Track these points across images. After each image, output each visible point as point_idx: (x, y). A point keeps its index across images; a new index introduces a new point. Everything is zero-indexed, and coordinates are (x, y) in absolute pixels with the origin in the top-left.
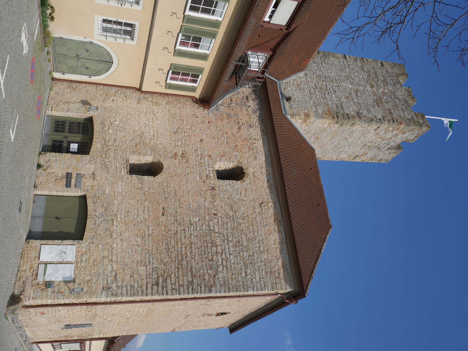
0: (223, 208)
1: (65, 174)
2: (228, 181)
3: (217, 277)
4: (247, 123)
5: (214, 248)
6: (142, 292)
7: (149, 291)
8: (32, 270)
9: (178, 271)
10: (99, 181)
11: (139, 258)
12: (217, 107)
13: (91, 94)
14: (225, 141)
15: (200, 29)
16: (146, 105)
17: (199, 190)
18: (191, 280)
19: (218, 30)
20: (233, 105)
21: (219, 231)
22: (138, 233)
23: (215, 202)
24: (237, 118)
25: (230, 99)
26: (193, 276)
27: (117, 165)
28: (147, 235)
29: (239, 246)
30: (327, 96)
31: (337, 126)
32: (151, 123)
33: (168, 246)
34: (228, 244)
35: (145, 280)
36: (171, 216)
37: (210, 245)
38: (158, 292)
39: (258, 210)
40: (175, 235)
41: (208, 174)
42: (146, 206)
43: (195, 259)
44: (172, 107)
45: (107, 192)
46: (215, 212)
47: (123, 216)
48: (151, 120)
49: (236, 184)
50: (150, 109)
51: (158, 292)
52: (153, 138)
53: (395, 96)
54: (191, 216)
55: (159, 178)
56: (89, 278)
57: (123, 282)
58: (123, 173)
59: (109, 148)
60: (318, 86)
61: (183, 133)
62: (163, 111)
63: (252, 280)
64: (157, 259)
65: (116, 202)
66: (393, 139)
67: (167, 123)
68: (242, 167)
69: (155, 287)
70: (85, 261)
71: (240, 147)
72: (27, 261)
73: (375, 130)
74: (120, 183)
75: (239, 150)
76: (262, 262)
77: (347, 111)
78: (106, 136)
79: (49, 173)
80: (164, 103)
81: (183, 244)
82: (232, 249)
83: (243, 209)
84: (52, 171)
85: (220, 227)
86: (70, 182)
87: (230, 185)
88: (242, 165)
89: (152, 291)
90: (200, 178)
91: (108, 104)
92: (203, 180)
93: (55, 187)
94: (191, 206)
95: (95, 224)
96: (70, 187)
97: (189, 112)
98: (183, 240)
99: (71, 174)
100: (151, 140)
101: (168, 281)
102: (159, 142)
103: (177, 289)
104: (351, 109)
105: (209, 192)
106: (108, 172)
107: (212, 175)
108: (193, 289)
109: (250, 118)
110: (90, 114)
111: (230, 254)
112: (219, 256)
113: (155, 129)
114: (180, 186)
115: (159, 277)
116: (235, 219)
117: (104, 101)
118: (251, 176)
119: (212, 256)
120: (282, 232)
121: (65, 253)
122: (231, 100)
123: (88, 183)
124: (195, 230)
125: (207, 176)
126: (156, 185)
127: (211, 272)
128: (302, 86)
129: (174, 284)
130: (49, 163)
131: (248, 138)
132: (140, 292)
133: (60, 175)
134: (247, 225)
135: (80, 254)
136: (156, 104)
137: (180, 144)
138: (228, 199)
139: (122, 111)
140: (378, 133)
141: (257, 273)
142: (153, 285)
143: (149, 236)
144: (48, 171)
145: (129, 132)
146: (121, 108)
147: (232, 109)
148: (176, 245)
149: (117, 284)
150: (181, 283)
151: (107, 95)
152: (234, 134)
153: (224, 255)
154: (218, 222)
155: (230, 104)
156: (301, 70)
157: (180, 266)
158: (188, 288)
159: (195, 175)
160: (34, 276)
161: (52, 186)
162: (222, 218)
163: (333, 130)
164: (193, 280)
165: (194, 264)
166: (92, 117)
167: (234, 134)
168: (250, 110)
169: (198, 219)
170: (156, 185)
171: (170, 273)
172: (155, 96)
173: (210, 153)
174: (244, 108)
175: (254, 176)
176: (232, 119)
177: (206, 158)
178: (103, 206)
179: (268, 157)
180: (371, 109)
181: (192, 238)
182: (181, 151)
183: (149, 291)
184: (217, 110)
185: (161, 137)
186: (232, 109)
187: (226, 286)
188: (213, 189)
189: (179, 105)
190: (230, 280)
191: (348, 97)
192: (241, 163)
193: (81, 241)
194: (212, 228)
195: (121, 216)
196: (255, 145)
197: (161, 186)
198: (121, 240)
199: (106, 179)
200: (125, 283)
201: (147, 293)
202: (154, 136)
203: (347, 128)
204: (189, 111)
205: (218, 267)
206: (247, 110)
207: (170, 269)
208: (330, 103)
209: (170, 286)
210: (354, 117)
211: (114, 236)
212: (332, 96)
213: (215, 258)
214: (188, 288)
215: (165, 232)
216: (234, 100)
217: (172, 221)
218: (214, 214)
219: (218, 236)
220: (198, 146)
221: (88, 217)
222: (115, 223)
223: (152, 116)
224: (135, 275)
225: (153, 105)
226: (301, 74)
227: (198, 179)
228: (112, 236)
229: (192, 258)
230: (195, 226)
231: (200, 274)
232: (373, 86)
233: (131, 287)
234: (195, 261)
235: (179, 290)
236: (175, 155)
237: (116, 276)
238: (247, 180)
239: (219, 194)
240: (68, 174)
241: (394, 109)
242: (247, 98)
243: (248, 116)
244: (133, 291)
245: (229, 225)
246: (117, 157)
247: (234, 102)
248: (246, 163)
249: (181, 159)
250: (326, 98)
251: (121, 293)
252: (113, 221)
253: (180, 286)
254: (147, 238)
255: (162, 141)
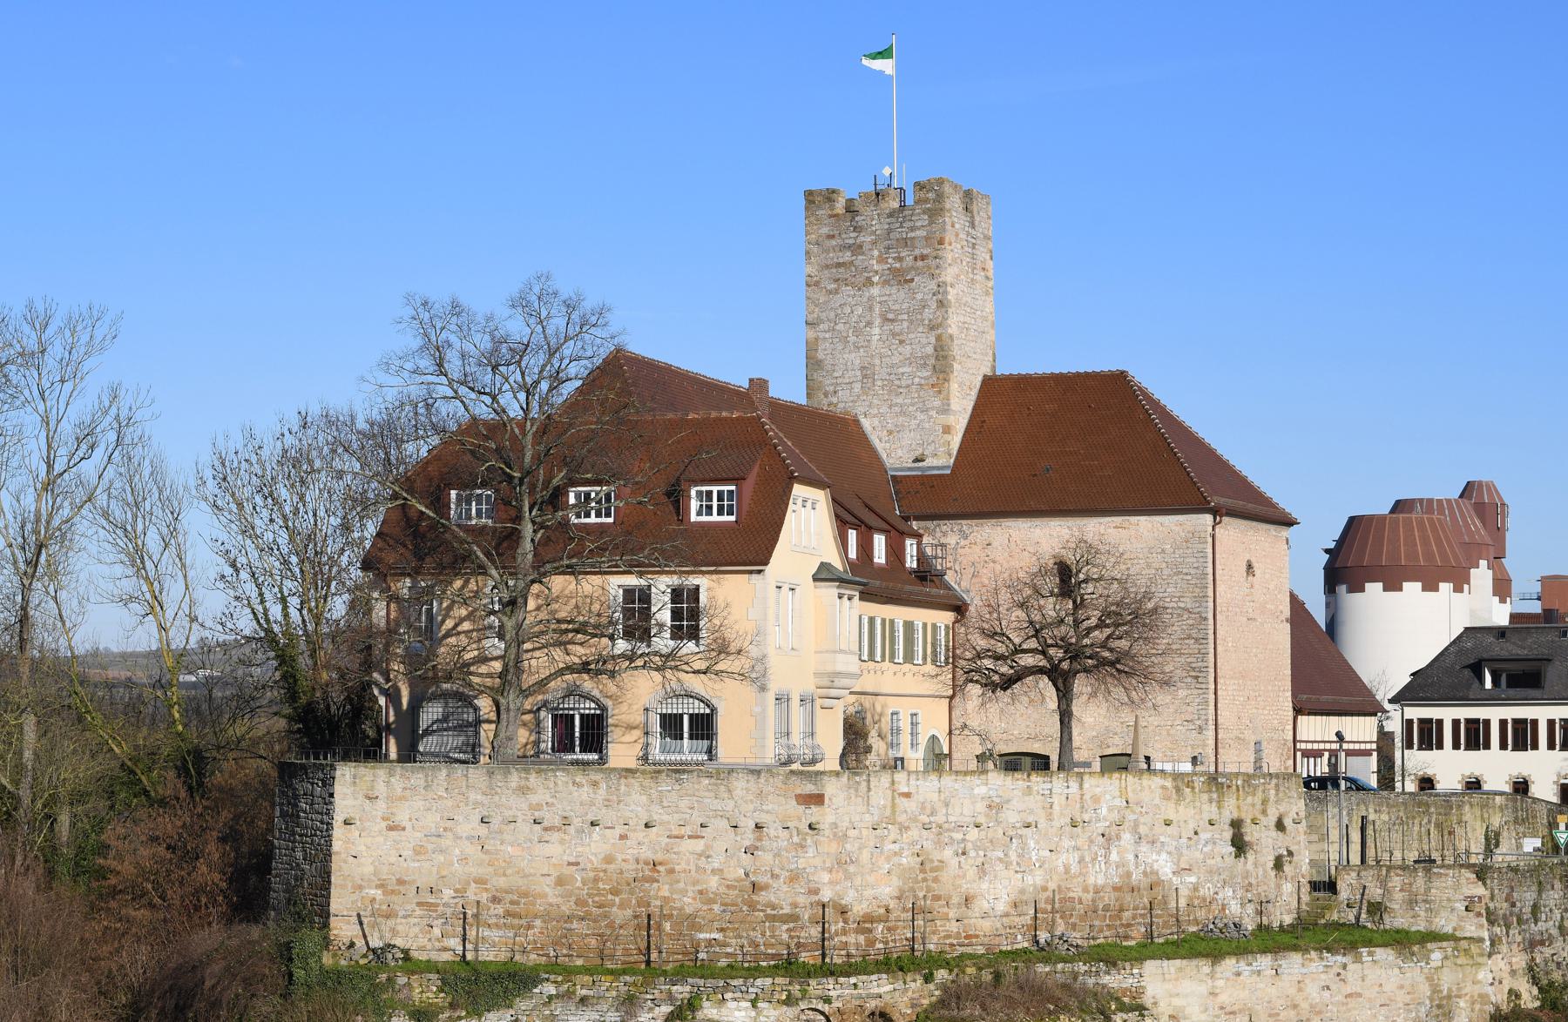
30: (904, 383)
77: (930, 350)
104: (924, 343)
156: (857, 422)
180: (919, 296)
191: (901, 342)
208: (917, 380)
210: (939, 338)
226: (866, 424)
232: (869, 279)
241: (914, 247)
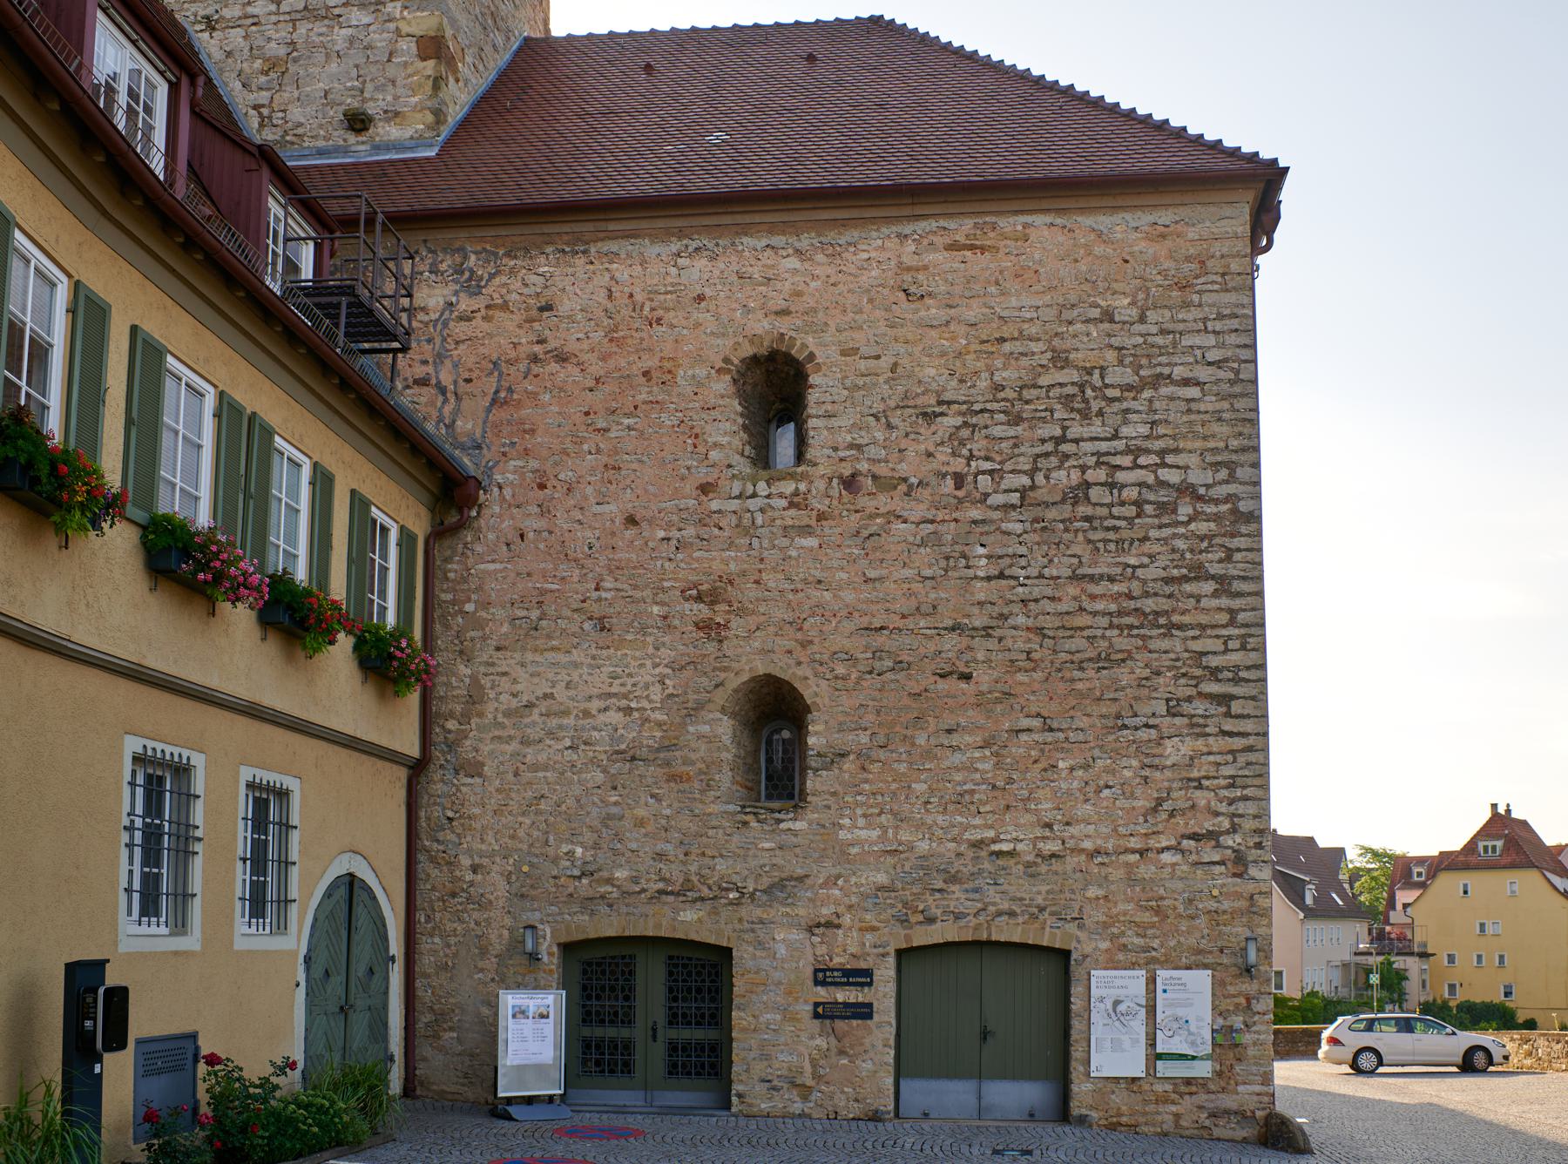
1: (817, 1022)
3: (1202, 491)
4: (530, 321)
5: (1094, 493)
6: (1250, 749)
7: (1248, 726)
8: (1173, 1096)
9: (1180, 627)
10: (841, 910)
11: (1135, 763)
13: (455, 955)
16: (481, 743)
17: (859, 541)
18: (1211, 582)
22: (1040, 766)
23: (905, 480)
26: (1198, 573)
27: (767, 845)
28: (1049, 737)
29: (1086, 401)
32: (569, 721)
33: (1090, 660)
34: (1076, 441)
35: (1211, 740)
36: (970, 648)
37: (1083, 510)
38: (1253, 698)
39: (934, 312)
40: (1044, 636)
41: (784, 503)
42: (933, 741)
43: (1134, 567)
44: (484, 638)
45: (882, 878)
46: (950, 482)
47: (977, 821)
48: (554, 722)
49: (822, 389)
50: (502, 726)
51: (1253, 698)
54: (970, 573)
55: (813, 690)
56: (1202, 922)
57: (1217, 814)
58: (799, 825)
59: (695, 879)
61: (604, 595)
63: (1209, 364)
64: (1136, 699)
65: (923, 846)
67: (562, 658)
68: (743, 361)
69: (1236, 707)
70: (1144, 936)
71: (650, 362)
72: (1145, 1114)
74: (842, 835)
75: (668, 365)
76: (1142, 319)
78: (644, 890)
79: (817, 1077)
80: (464, 670)
81: (1081, 609)
82: (1096, 429)
83: (932, 372)
84: (808, 1068)
85: (1008, 466)
86: (846, 1005)
88: (736, 362)
89: (1249, 716)
90: (806, 530)
91: (496, 886)
92: (813, 522)
93: (871, 1054)
94: (928, 573)
95: (1012, 914)
96: (870, 1005)
97: (498, 566)
98: (1063, 607)
99: (816, 1005)
100: (647, 720)
101: (1214, 661)
102: (658, 687)
103: (1243, 631)
106: (801, 879)
108: (1244, 578)
109: (505, 307)
110: (550, 954)
111: (1115, 437)
112: (1121, 476)
113: (595, 705)
114: (844, 613)
115: (1200, 694)
116: (977, 407)
117: (483, 904)
118: (784, 325)
119: (1122, 504)
121: (1117, 1003)
123: (847, 948)
124: (1023, 562)
125: (792, 505)
126: (847, 702)
127: (1184, 511)
129: (1225, 643)
130: (775, 1083)
131: (606, 322)
132: (1252, 757)
133: (821, 1042)
135: (1121, 957)
136: (475, 698)
137: (656, 609)
139: (521, 833)
141: (1187, 341)
142: (1228, 714)
143: (1051, 730)
144: (809, 1082)
145: (616, 804)
146: (512, 837)
147: (469, 381)
148: (1086, 633)
149: (1227, 832)
150: (1223, 618)
151: (454, 895)
152: (592, 383)
153: (1118, 460)
155: (443, 391)
157: (1162, 621)
158: (1239, 595)
159: (794, 553)
160: (1194, 1089)
161: (868, 1065)
164: (1213, 577)
165: (1153, 572)
166: (559, 945)
167: (592, 383)
170: (847, 702)
171: (1186, 655)
173: (689, 487)
174: (460, 329)
175: (784, 312)
176: (518, 388)
177: (714, 505)
178: (939, 891)
179: (694, 245)
181: (1055, 573)
182: (687, 605)
183: (1248, 726)
184: (479, 447)
186: (469, 381)
187: (1234, 457)
188: (850, 483)
189: (469, 607)
190: (1211, 444)
192: (726, 360)
193: (1074, 956)
194: (1014, 498)
195: (975, 827)
196: (639, 297)
197: (850, 684)
198: (1068, 824)
199: (831, 881)
200: (1223, 808)
201: (1257, 734)
202: (628, 711)
204: (492, 567)
205: (1162, 484)
207: (1172, 656)
209: (1235, 658)
211: (1051, 847)
213: (1131, 493)
214: (1239, 595)
215: (1034, 670)
217: (992, 644)
218: (958, 486)
219: (1047, 477)
220: (661, 534)
221: (984, 937)
222: (1005, 847)
223: (535, 716)
224: (1195, 774)
225: (481, 715)
227: (811, 542)
228: (1053, 855)
229: (1133, 576)
230: (1007, 561)
231: (1192, 551)
233: (1232, 786)
234: (1142, 566)
235: (1247, 626)
237: (1195, 837)
238: (804, 346)
240: (816, 1016)
243: (498, 314)
244: (1249, 781)
246: (732, 847)
247: (430, 369)
248: (729, 343)
251: (1255, 817)
252: (999, 854)
253: (1232, 622)
254: (1061, 735)
255: (648, 678)
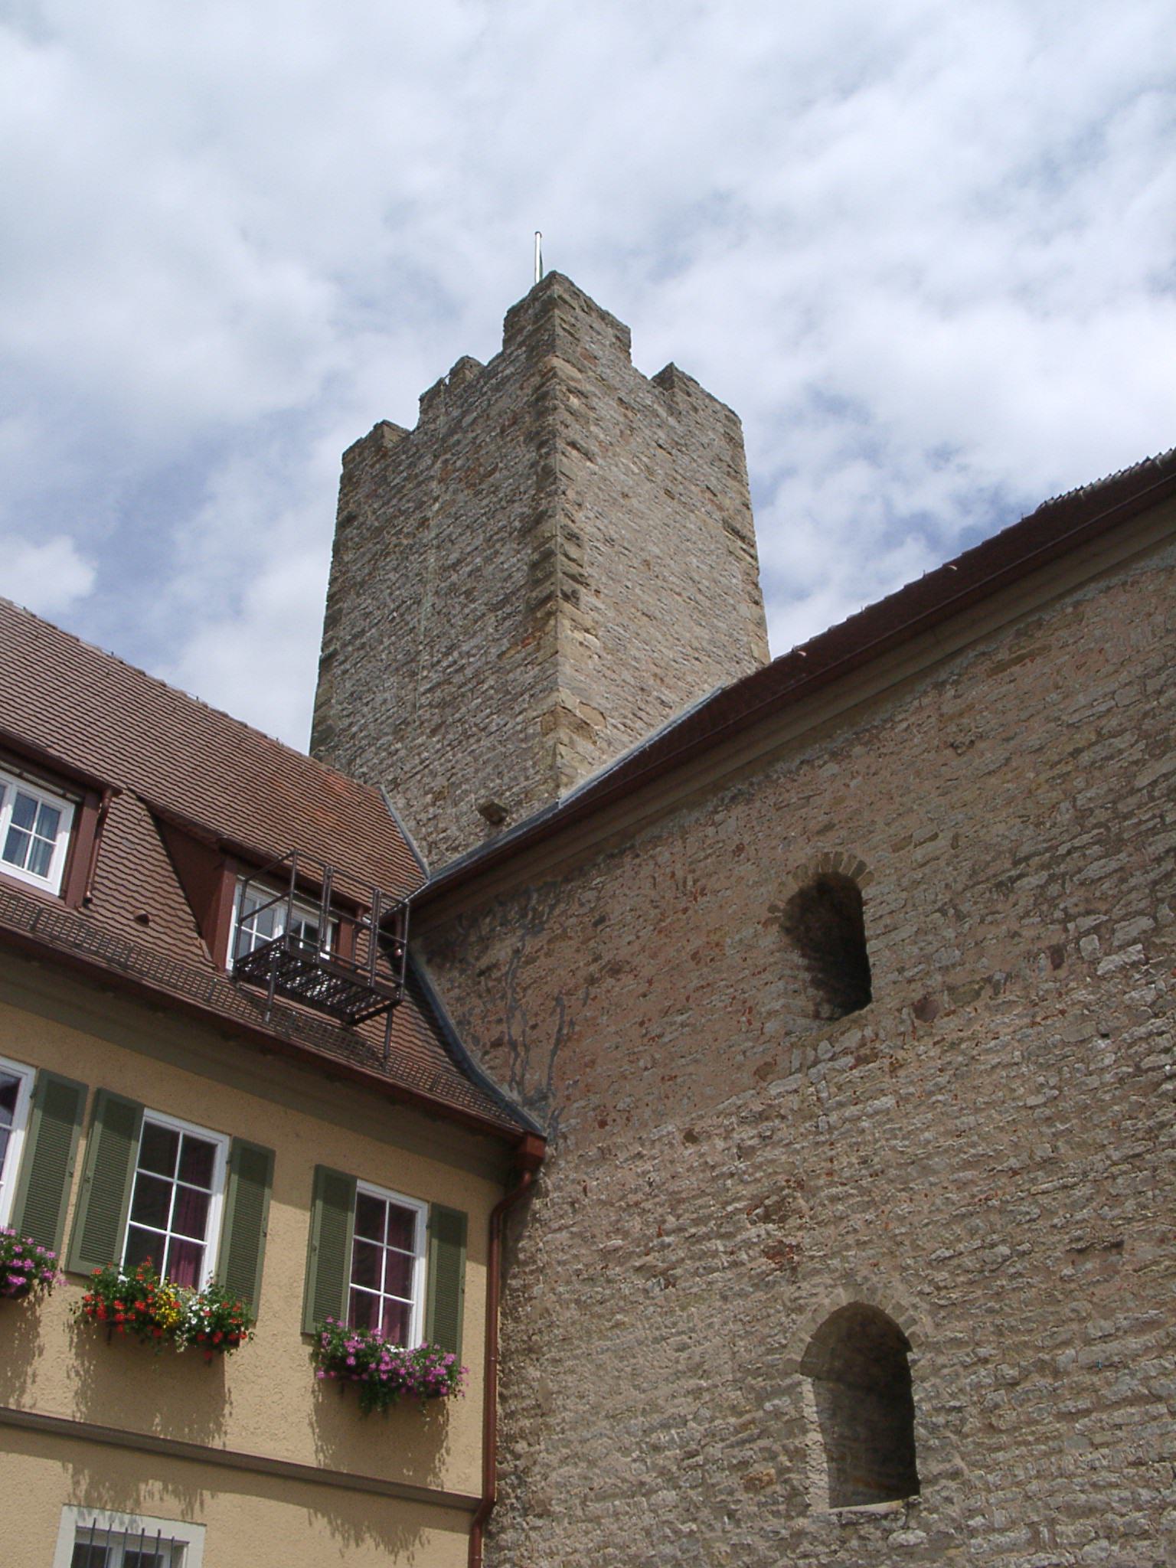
0: (1015, 927)
2: (870, 947)
12: (530, 1103)
14: (679, 1019)
15: (85, 1180)
16: (553, 1471)
19: (92, 1089)
20: (516, 1031)
21: (1141, 913)
23: (989, 980)
24: (569, 993)
25: (494, 1053)
30: (469, 672)
31: (586, 597)
39: (990, 754)
41: (850, 1060)
46: (1044, 961)
49: (878, 899)
52: (706, 1397)
53: (452, 432)
60: (437, 720)
61: (667, 1240)
62: (572, 1372)
66: (622, 395)
68: (791, 901)
71: (697, 942)
73: (588, 456)
75: (715, 938)
80: (533, 1373)
83: (1001, 828)
85: (1117, 912)
87: (889, 930)
104: (514, 560)
105: (947, 1026)
107: (852, 1039)
109: (564, 936)
113: (665, 1389)
116: (1063, 850)
118: (827, 844)
120: (1076, 605)
122: (497, 1044)
125: (861, 1061)
128: (440, 782)
131: (653, 913)
134: (1079, 782)
136: (540, 1410)
137: (719, 1245)
138: (960, 917)
140: (605, 448)
147: (534, 1027)
154: (1096, 929)
155: (513, 1045)
162: (1069, 917)
163: (611, 614)
168: (530, 946)
169: (1102, 1044)
172: (505, 1427)
174: (526, 975)
175: (829, 827)
177: (774, 1091)
179: (729, 794)
184: (545, 1098)
185: (699, 1349)
186: (534, 1027)
194: (1135, 952)
196: (680, 874)
203: (592, 560)
206: (534, 960)
212: (469, 654)
216: (496, 1032)
218: (1057, 966)
227: (888, 1101)
236: (776, 1252)
238: (853, 857)
239: (945, 970)
242: (482, 973)
245: (1094, 870)
247: (504, 1027)
249: (793, 1222)
250: (476, 675)
